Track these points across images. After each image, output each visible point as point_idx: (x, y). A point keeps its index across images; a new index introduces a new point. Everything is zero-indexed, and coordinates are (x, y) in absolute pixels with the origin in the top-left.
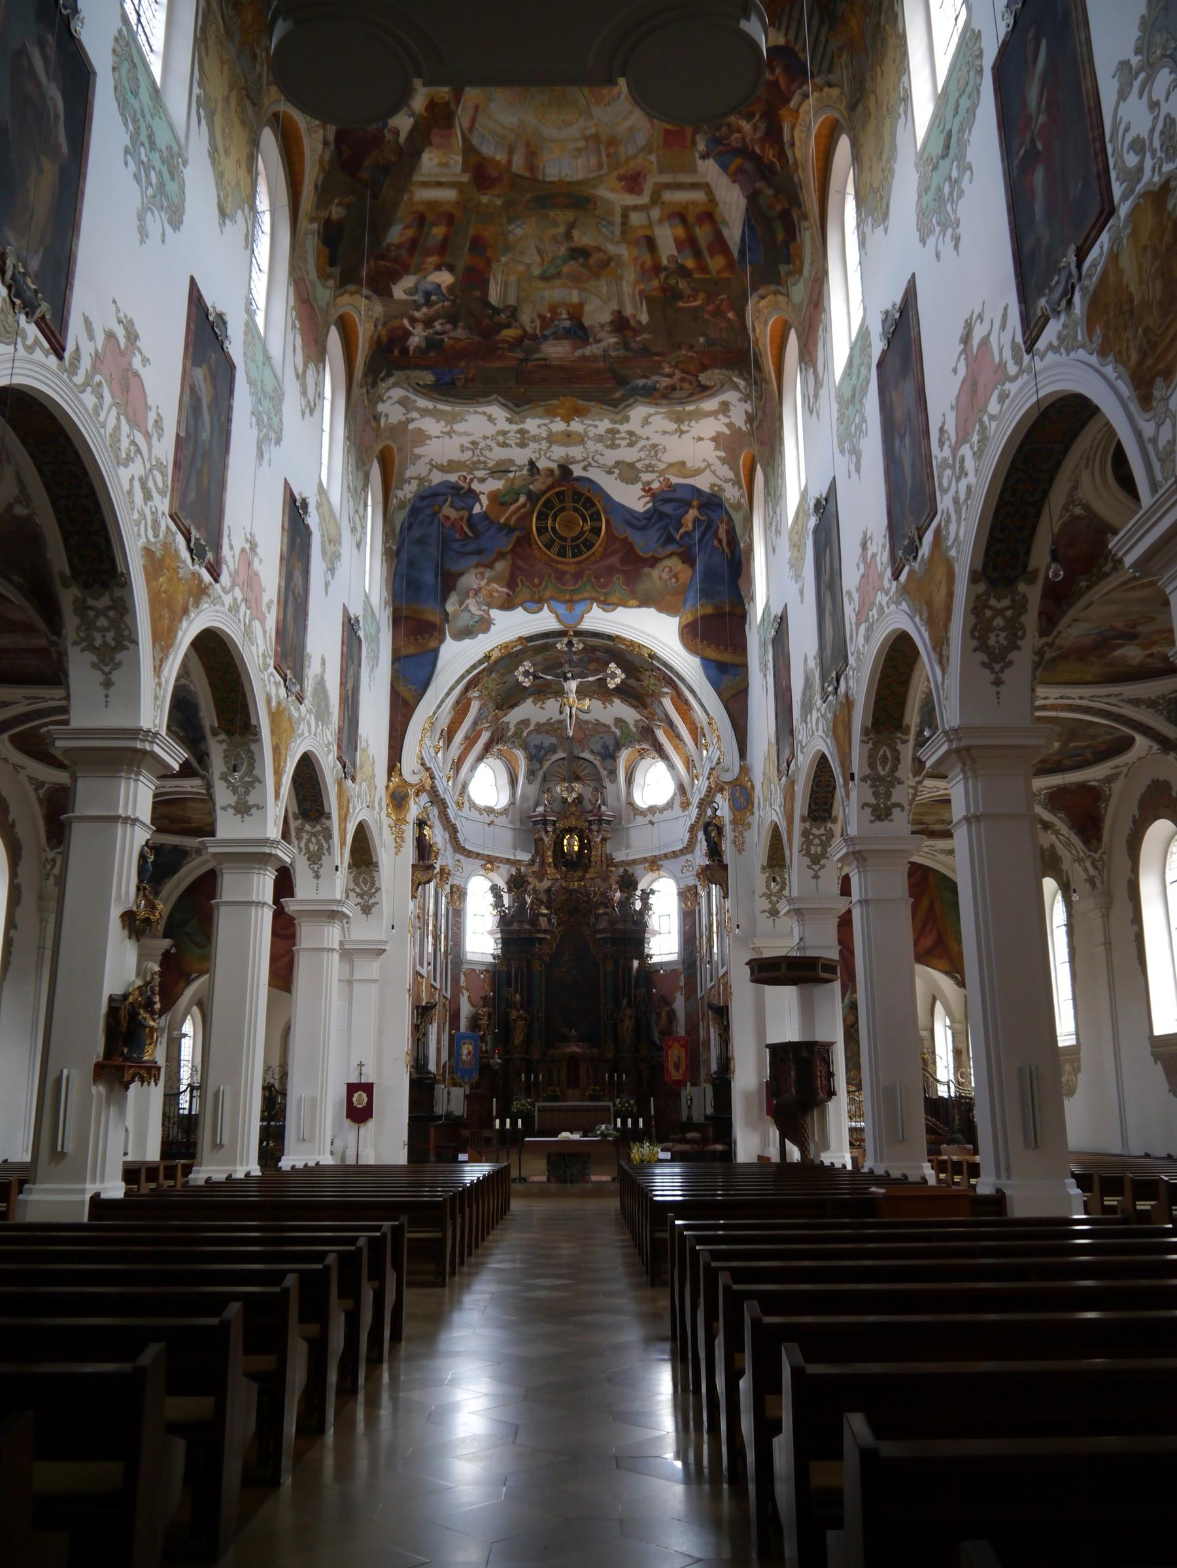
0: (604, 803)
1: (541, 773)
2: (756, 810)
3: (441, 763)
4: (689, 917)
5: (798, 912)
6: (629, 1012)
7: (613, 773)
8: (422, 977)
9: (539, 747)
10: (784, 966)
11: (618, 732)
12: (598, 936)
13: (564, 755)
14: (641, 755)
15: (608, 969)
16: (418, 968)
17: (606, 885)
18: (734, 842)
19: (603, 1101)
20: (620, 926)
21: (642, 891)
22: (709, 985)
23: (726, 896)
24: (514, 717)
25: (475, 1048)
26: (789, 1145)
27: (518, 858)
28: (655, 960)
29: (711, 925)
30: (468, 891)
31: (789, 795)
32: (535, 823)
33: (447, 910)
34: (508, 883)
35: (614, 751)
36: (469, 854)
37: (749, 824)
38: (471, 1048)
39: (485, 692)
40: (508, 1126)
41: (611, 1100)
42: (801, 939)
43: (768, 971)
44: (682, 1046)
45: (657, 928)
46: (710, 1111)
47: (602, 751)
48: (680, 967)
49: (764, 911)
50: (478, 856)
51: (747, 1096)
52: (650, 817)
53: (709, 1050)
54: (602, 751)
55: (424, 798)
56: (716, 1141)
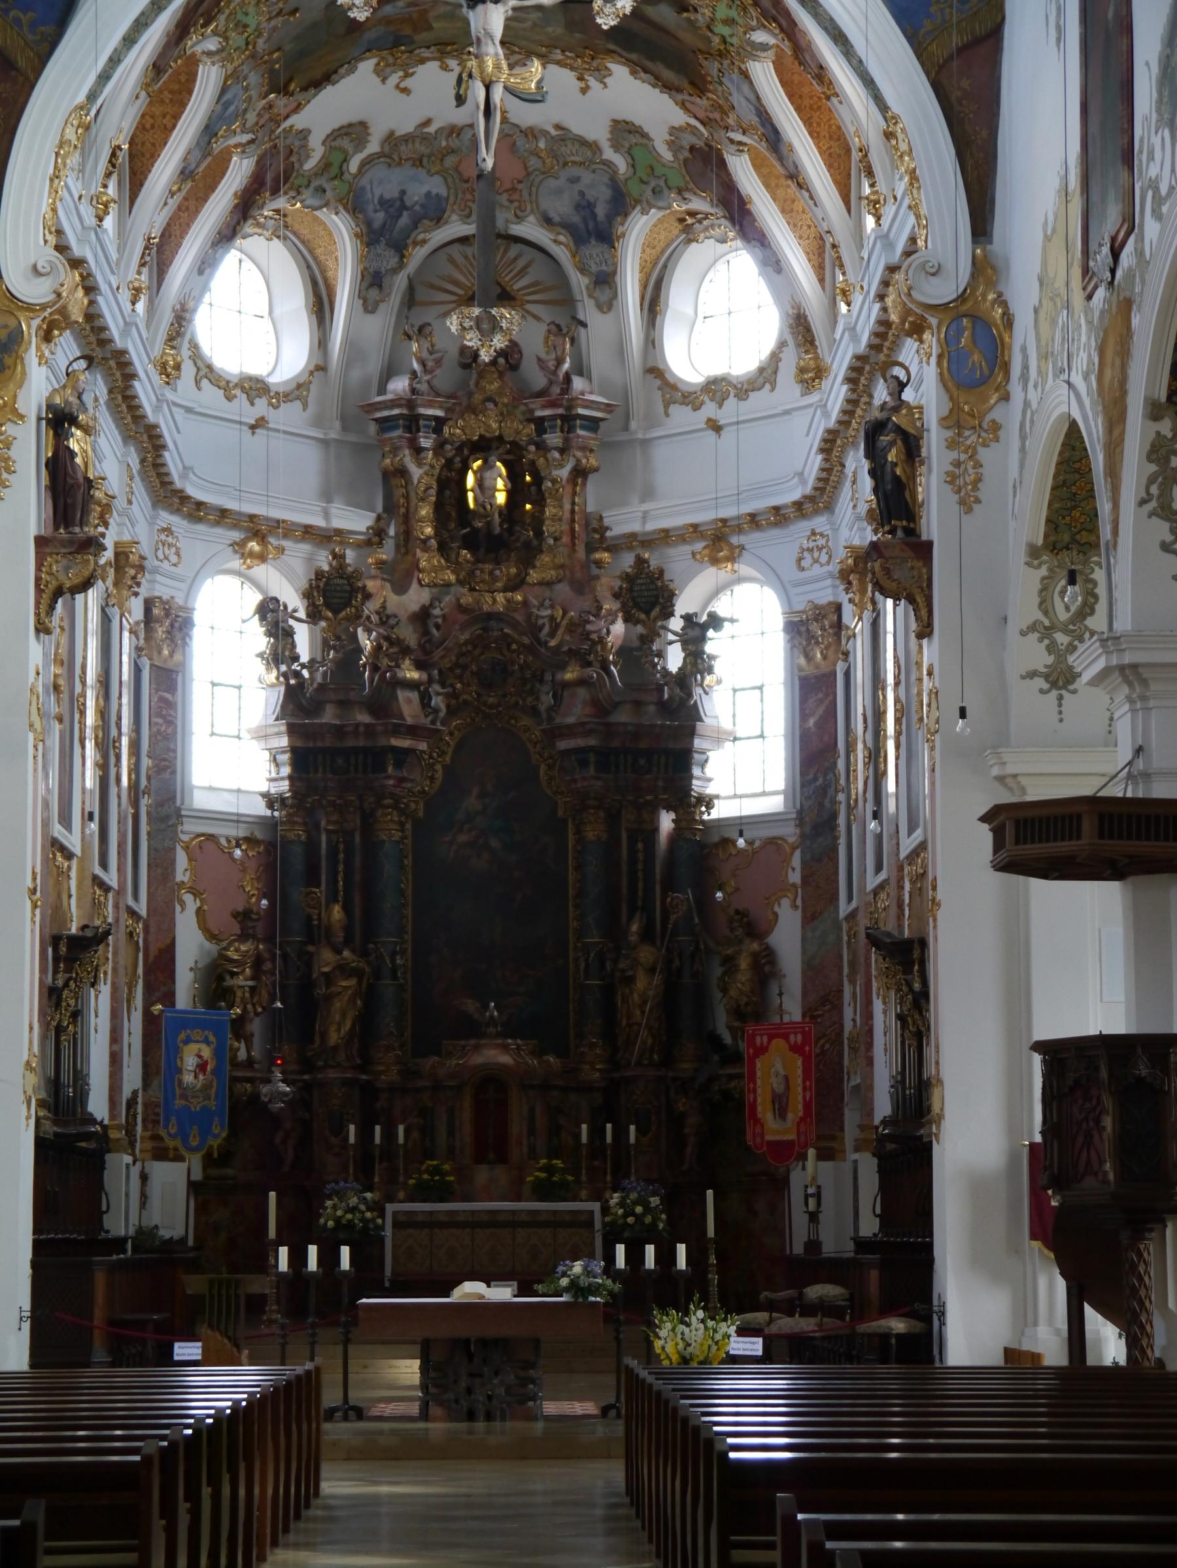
0: (580, 369)
1: (400, 282)
2: (1015, 387)
3: (113, 248)
4: (817, 695)
5: (1132, 674)
6: (646, 954)
7: (605, 281)
8: (69, 856)
9: (395, 206)
10: (1088, 826)
11: (621, 163)
12: (563, 745)
13: (469, 229)
14: (687, 229)
15: (590, 835)
16: (58, 830)
17: (586, 603)
18: (951, 479)
19: (575, 1198)
20: (622, 717)
21: (688, 618)
22: (872, 882)
23: (925, 631)
24: (320, 114)
25: (218, 1053)
26: (1092, 1317)
27: (337, 523)
28: (721, 811)
29: (879, 715)
30: (198, 617)
31: (1116, 340)
32: (385, 424)
33: (137, 670)
34: (307, 595)
35: (610, 218)
36: (196, 511)
37: (996, 427)
38: (206, 1052)
39: (237, 39)
40: (313, 1264)
41: (597, 1196)
42: (1139, 751)
43: (1043, 839)
44: (795, 1049)
45: (726, 724)
46: (869, 1227)
47: (576, 219)
48: (790, 832)
49: (1032, 674)
50: (223, 516)
51: (977, 1187)
52: (709, 409)
53: (870, 1062)
54: (576, 219)
55: (67, 347)
56: (887, 1310)
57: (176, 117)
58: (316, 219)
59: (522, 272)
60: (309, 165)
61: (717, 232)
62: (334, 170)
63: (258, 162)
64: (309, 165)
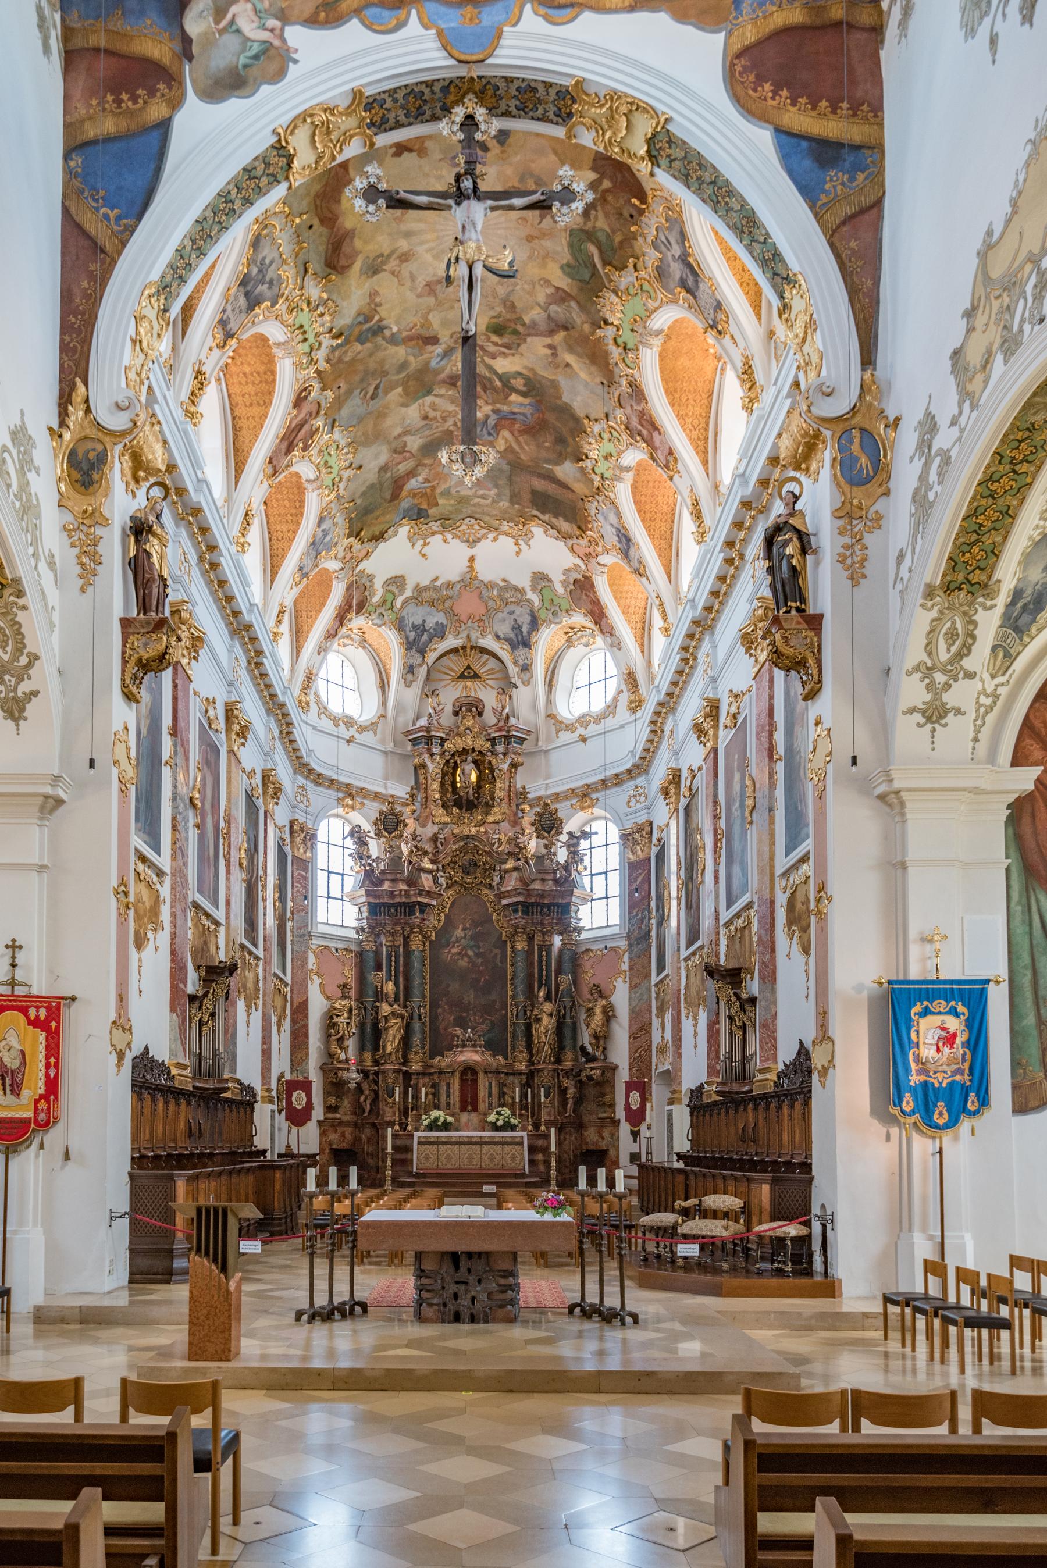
7: (526, 668)
35: (529, 634)
47: (512, 635)
54: (512, 635)
57: (295, 532)
58: (380, 634)
59: (484, 664)
60: (376, 599)
61: (584, 640)
62: (388, 605)
63: (348, 589)
64: (376, 599)
